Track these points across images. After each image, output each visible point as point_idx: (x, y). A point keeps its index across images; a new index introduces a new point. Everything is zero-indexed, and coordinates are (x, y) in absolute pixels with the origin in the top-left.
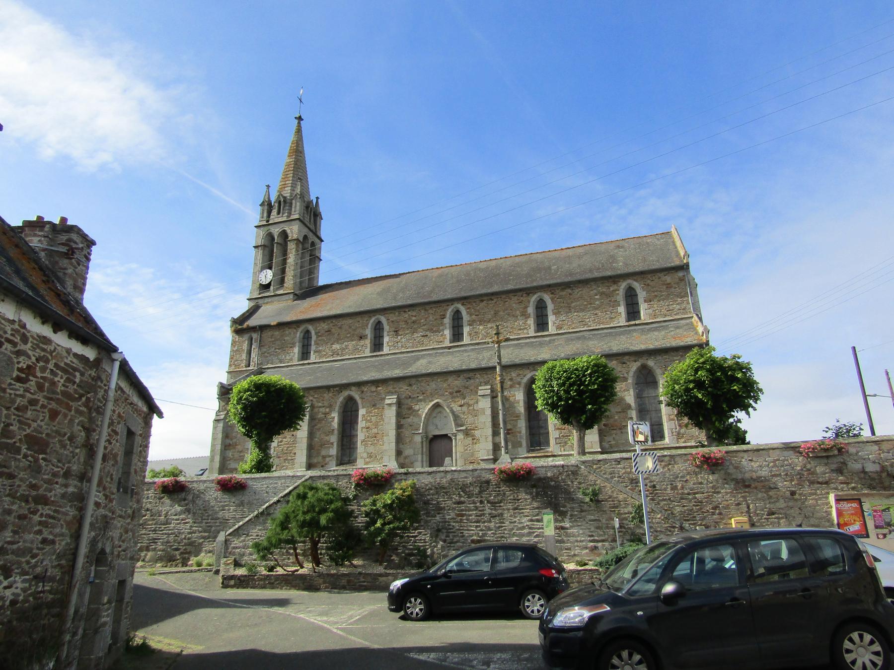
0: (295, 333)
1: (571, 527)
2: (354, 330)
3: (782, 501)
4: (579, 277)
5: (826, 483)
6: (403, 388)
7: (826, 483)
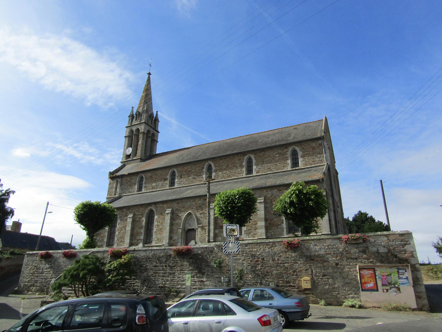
0: (136, 178)
1: (206, 281)
2: (162, 176)
3: (330, 268)
4: (269, 145)
5: (356, 259)
6: (175, 205)
7: (356, 259)
